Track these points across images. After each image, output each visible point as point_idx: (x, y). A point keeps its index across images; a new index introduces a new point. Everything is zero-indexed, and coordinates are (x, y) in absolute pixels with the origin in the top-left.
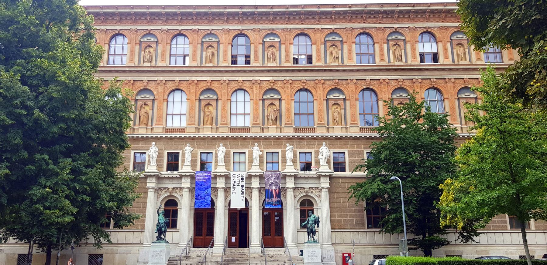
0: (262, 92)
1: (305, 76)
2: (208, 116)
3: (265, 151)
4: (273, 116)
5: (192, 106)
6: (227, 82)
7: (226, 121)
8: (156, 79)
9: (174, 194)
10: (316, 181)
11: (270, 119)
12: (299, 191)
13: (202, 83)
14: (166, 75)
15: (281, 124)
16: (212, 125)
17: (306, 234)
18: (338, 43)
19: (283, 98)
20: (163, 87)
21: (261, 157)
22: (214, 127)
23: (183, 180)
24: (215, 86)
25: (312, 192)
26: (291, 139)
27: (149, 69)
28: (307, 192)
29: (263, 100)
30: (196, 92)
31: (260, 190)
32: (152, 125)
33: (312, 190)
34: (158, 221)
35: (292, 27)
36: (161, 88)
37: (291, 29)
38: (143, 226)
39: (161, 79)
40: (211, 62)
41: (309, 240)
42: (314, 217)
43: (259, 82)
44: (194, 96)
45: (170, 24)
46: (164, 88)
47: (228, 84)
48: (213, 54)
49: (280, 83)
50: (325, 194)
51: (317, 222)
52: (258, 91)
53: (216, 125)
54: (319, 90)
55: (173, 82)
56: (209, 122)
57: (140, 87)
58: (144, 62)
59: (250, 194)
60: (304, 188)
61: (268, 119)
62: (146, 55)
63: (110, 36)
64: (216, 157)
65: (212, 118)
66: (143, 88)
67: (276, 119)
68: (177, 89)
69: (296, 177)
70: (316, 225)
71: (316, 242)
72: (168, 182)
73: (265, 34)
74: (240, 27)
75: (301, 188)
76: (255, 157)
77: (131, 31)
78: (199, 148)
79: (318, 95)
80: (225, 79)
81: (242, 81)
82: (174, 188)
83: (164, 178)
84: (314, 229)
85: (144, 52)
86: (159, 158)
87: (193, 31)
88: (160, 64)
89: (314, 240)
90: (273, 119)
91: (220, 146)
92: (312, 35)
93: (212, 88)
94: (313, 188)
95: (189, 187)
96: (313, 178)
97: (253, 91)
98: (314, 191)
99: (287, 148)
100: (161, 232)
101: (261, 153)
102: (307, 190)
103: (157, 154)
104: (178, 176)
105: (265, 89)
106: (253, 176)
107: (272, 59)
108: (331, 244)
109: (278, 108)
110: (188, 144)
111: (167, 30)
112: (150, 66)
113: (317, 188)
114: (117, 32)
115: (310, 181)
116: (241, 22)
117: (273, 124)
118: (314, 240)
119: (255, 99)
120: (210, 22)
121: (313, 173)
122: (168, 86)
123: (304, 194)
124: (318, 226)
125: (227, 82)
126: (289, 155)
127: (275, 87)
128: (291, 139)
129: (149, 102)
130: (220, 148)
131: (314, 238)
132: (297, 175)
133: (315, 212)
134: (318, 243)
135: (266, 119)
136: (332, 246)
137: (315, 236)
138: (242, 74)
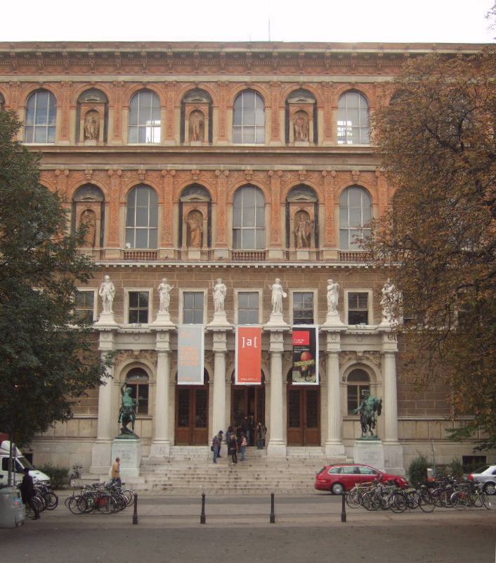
0: (286, 191)
1: (358, 165)
2: (194, 230)
3: (291, 292)
4: (304, 233)
5: (168, 215)
6: (227, 173)
7: (224, 240)
8: (107, 167)
9: (143, 361)
10: (375, 341)
11: (300, 236)
12: (347, 358)
13: (182, 175)
14: (123, 160)
15: (317, 245)
16: (202, 246)
17: (358, 425)
19: (321, 200)
20: (117, 181)
21: (285, 301)
22: (205, 249)
23: (158, 338)
24: (206, 181)
25: (368, 358)
26: (334, 272)
27: (95, 151)
28: (360, 358)
29: (288, 204)
30: (174, 191)
31: (284, 354)
32: (101, 245)
33: (368, 356)
34: (123, 404)
35: (336, 79)
36: (115, 181)
37: (334, 83)
38: (96, 410)
39: (115, 167)
40: (198, 139)
41: (364, 435)
42: (374, 400)
43: (280, 173)
45: (128, 73)
46: (120, 183)
47: (227, 177)
48: (202, 125)
49: (316, 175)
50: (390, 365)
51: (378, 407)
52: (279, 189)
53: (209, 245)
54: (381, 189)
55: (135, 173)
56: (197, 241)
57: (81, 181)
58: (86, 138)
59: (267, 362)
60: (355, 352)
61: (296, 237)
62: (88, 127)
63: (27, 93)
64: (211, 300)
65: (202, 233)
66: (84, 182)
67: (309, 238)
69: (343, 334)
70: (376, 412)
71: (376, 438)
72: (130, 339)
73: (289, 91)
74: (247, 78)
75: (350, 351)
76: (275, 302)
77: (62, 85)
78: (182, 286)
79: (380, 197)
80: (222, 167)
81: (251, 172)
82: (141, 351)
83: (126, 334)
84: (373, 419)
85: (85, 120)
86: (118, 299)
87: (167, 85)
89: (372, 434)
90: (304, 237)
91: (216, 283)
92: (369, 94)
93: (200, 182)
94: (369, 351)
95: (168, 350)
96: (370, 335)
97: (270, 189)
98: (371, 357)
99: (329, 287)
100: (126, 417)
101: (285, 295)
102: (360, 354)
103: (113, 294)
104: (148, 331)
105: (291, 186)
106: (273, 332)
107: (302, 134)
108: (396, 440)
109: (312, 217)
110: (164, 279)
111: (122, 83)
112: (95, 145)
113: (376, 351)
114: (38, 87)
115: (367, 341)
116: (248, 70)
117: (304, 246)
118: (372, 434)
119: (273, 203)
120: (195, 69)
121: (370, 327)
122: (126, 180)
123: (354, 362)
124: (379, 414)
125: (227, 173)
126: (332, 298)
127: (307, 183)
128: (334, 272)
129: (95, 207)
130: (217, 286)
131: (371, 432)
132: (345, 331)
133: (372, 390)
134: (379, 440)
135: (292, 236)
136: (397, 443)
137: (373, 428)
138: (252, 160)
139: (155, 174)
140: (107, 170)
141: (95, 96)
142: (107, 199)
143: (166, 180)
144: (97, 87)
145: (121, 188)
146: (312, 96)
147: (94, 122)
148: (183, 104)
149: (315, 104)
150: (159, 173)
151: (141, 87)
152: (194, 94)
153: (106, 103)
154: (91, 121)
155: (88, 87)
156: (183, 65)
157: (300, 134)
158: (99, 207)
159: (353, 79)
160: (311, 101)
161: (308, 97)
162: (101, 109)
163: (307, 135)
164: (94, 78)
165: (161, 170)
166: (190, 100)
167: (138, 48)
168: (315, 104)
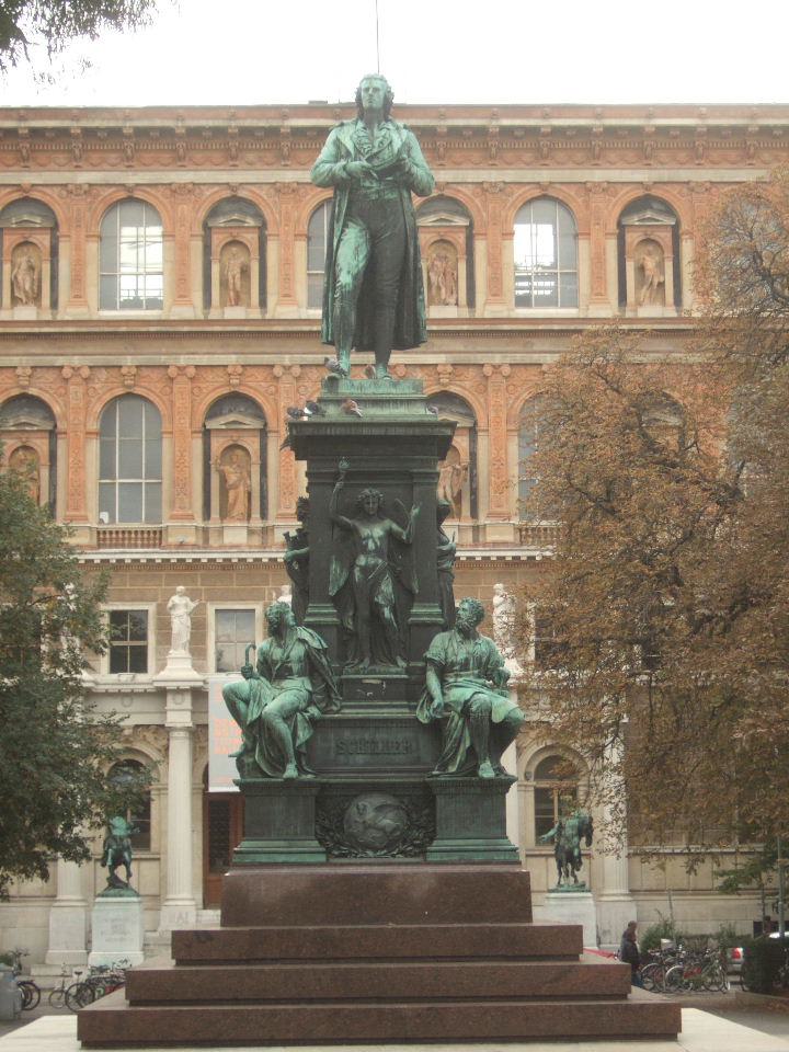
8: (60, 361)
18: (663, 234)
20: (81, 390)
27: (36, 330)
35: (510, 175)
39: (76, 361)
44: (188, 421)
55: (114, 372)
58: (15, 300)
62: (20, 278)
68: (129, 395)
85: (13, 266)
87: (174, 190)
88: (67, 312)
92: (577, 203)
129: (38, 442)
139: (155, 375)
140: (61, 367)
141: (32, 214)
142: (61, 426)
143: (176, 387)
144: (35, 195)
145: (89, 402)
146: (465, 213)
147: (31, 268)
148: (207, 229)
149: (470, 228)
150: (162, 371)
151: (123, 194)
152: (227, 207)
153: (55, 228)
154: (24, 266)
155: (16, 196)
156: (206, 149)
157: (439, 288)
158: (46, 441)
159: (544, 176)
160: (461, 222)
161: (456, 213)
162: (44, 240)
163: (453, 291)
164: (28, 178)
165: (168, 367)
166: (221, 221)
167: (117, 119)
168: (470, 228)
